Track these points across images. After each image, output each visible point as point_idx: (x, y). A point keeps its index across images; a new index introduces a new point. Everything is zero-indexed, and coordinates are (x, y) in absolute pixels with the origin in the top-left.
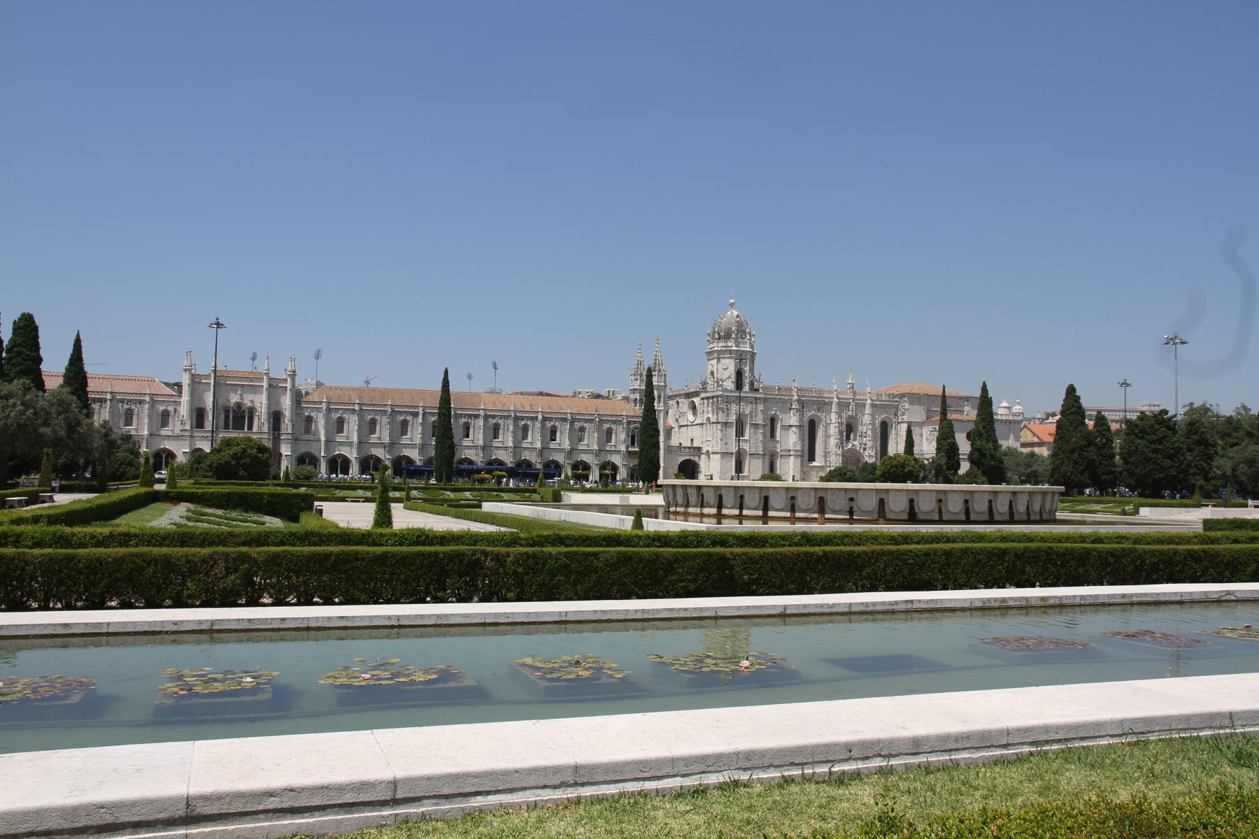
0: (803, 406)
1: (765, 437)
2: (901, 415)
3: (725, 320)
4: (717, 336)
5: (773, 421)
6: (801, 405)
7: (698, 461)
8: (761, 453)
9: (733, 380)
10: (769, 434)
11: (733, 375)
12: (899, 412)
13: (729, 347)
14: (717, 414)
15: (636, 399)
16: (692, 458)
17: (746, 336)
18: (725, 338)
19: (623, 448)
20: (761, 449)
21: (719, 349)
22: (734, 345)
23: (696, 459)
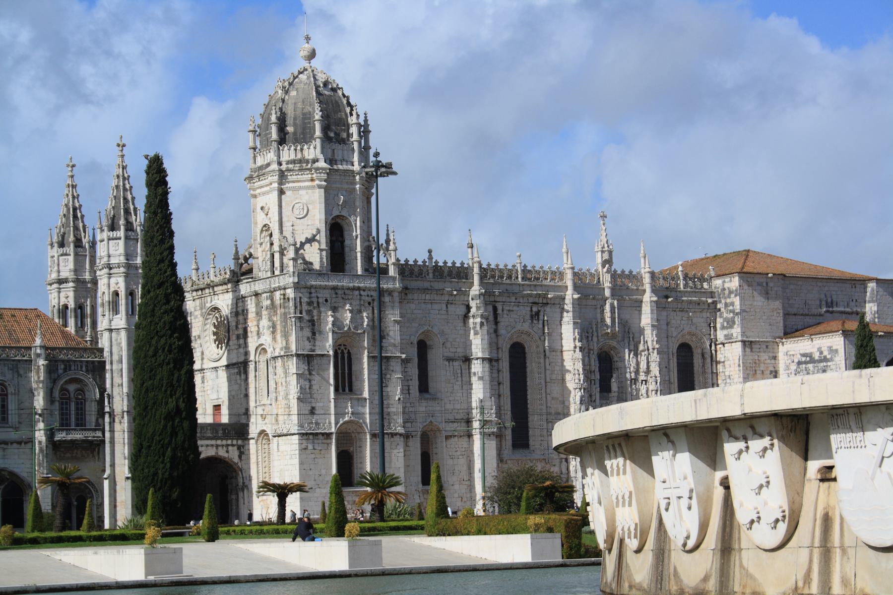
0: (495, 309)
1: (406, 390)
2: (723, 328)
3: (293, 93)
4: (274, 135)
5: (423, 348)
6: (490, 308)
7: (236, 460)
8: (400, 430)
9: (324, 246)
10: (415, 384)
11: (323, 233)
12: (719, 321)
13: (307, 162)
14: (286, 336)
15: (66, 307)
16: (222, 453)
17: (349, 135)
18: (296, 141)
19: (40, 436)
20: (400, 420)
21: (284, 167)
22: (321, 157)
23: (233, 454)
